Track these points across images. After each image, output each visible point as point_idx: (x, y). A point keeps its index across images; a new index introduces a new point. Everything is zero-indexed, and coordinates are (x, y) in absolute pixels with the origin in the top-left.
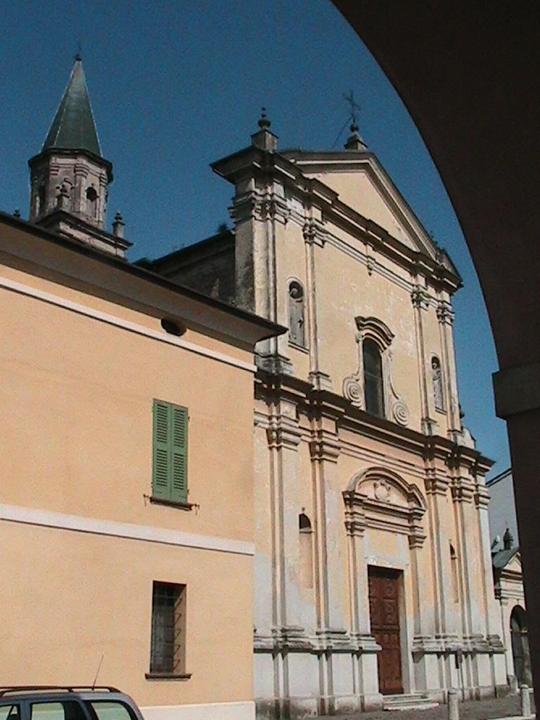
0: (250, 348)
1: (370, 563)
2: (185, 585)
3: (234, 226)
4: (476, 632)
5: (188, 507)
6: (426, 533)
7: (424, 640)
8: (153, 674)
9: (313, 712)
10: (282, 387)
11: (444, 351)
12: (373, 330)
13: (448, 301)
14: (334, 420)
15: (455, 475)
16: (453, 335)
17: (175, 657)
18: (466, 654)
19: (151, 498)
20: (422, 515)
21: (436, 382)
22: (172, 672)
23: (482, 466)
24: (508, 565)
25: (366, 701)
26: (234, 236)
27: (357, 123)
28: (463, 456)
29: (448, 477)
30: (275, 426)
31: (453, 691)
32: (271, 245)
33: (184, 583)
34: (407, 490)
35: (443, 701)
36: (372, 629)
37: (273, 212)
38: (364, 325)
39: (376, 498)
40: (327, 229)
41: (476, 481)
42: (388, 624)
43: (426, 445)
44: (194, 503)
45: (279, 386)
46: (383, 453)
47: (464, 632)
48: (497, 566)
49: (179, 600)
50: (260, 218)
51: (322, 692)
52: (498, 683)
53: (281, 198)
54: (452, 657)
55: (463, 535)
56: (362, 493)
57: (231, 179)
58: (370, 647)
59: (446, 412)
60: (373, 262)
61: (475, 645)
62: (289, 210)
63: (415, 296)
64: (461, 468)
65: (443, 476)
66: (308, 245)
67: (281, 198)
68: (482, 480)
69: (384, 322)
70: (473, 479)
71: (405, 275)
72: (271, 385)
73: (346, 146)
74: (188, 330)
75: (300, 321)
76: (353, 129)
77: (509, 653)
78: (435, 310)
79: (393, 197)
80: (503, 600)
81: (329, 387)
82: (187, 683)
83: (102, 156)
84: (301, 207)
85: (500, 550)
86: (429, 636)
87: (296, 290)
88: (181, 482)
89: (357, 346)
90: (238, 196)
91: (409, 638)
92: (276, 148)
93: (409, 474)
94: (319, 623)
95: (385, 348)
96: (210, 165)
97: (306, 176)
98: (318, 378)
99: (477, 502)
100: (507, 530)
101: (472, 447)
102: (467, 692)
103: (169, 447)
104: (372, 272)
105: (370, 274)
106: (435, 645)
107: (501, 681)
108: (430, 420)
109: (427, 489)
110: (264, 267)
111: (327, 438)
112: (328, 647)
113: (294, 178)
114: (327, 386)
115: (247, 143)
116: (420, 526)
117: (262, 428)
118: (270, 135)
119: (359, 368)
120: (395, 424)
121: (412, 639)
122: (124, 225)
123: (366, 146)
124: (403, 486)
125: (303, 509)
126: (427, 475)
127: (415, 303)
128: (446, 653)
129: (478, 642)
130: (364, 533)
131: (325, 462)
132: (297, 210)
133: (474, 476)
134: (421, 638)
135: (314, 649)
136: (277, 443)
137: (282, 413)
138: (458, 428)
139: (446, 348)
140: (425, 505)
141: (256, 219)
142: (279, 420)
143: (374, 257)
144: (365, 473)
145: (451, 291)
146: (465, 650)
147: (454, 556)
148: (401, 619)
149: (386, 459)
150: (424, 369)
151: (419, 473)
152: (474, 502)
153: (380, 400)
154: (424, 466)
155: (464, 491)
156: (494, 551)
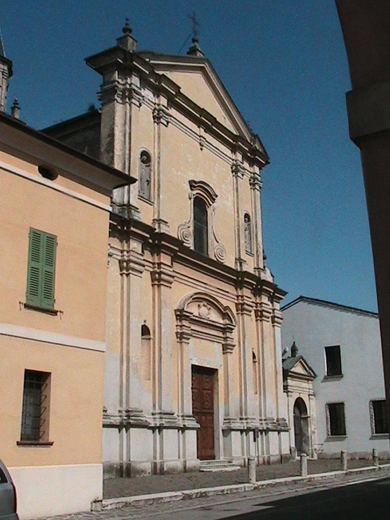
0: (109, 193)
1: (193, 364)
2: (50, 373)
3: (101, 106)
4: (269, 416)
5: (55, 313)
6: (235, 342)
7: (231, 421)
8: (22, 442)
9: (148, 472)
10: (132, 229)
11: (253, 210)
12: (202, 191)
13: (258, 173)
14: (170, 255)
15: (258, 301)
16: (261, 198)
17: (41, 429)
18: (261, 431)
19: (25, 304)
20: (233, 329)
21: (247, 232)
22: (38, 440)
23: (278, 295)
24: (293, 368)
25: (187, 463)
26: (101, 114)
27: (197, 37)
28: (264, 287)
29: (253, 302)
30: (126, 258)
31: (252, 458)
32: (128, 121)
33: (49, 371)
34: (223, 310)
35: (243, 465)
36: (193, 412)
37: (131, 97)
38: (195, 187)
39: (200, 315)
40: (171, 114)
41: (273, 306)
42: (205, 409)
43: (238, 278)
44: (59, 310)
45: (130, 228)
46: (206, 282)
47: (261, 415)
48: (285, 369)
49: (45, 385)
50: (121, 102)
51: (155, 458)
52: (283, 453)
53: (137, 87)
54: (251, 433)
55: (263, 345)
56: (189, 311)
57: (101, 70)
58: (191, 425)
59: (253, 255)
60: (204, 140)
61: (268, 425)
62: (143, 97)
63: (234, 167)
64: (263, 296)
65: (250, 302)
66: (156, 124)
67: (137, 87)
68: (277, 306)
69: (210, 185)
70: (271, 304)
71: (228, 152)
72: (123, 225)
73: (188, 53)
74: (59, 176)
75: (148, 181)
76: (194, 41)
77: (292, 431)
78: (248, 179)
79: (223, 97)
80: (289, 394)
81: (168, 231)
82: (49, 448)
83: (5, 56)
84: (152, 96)
85: (288, 357)
86: (236, 418)
87: (146, 157)
88: (49, 293)
89: (190, 201)
90: (105, 83)
91: (220, 419)
92: (135, 48)
93: (224, 298)
94: (154, 406)
95: (210, 205)
96: (85, 60)
97: (157, 72)
98: (159, 224)
99: (273, 322)
100: (294, 343)
101: (272, 282)
102: (261, 459)
103: (42, 266)
104: (203, 148)
105: (201, 149)
106: (239, 424)
107: (286, 451)
108: (242, 259)
109: (237, 311)
110: (122, 138)
111: (164, 269)
112: (160, 425)
113: (148, 73)
114: (166, 230)
115: (114, 44)
116: (230, 337)
117: (116, 259)
118: (131, 40)
119: (190, 218)
120: (215, 261)
121: (223, 420)
122: (19, 108)
123: (203, 55)
124: (220, 308)
125: (145, 321)
126: (238, 300)
127: (234, 173)
128: (247, 430)
129: (271, 423)
130: (189, 341)
131: (162, 287)
132: (149, 98)
133: (272, 303)
134: (229, 419)
135: (150, 425)
136: (127, 271)
137: (131, 249)
138: (261, 266)
139: (255, 208)
140: (236, 323)
141: (117, 102)
142: (129, 254)
143: (204, 136)
144: (191, 297)
145: (261, 167)
146: (261, 429)
147: (255, 360)
148: (215, 405)
149: (207, 287)
150: (238, 222)
151: (233, 298)
152: (271, 322)
153: (206, 243)
154: (235, 293)
155: (264, 313)
156: (284, 358)
